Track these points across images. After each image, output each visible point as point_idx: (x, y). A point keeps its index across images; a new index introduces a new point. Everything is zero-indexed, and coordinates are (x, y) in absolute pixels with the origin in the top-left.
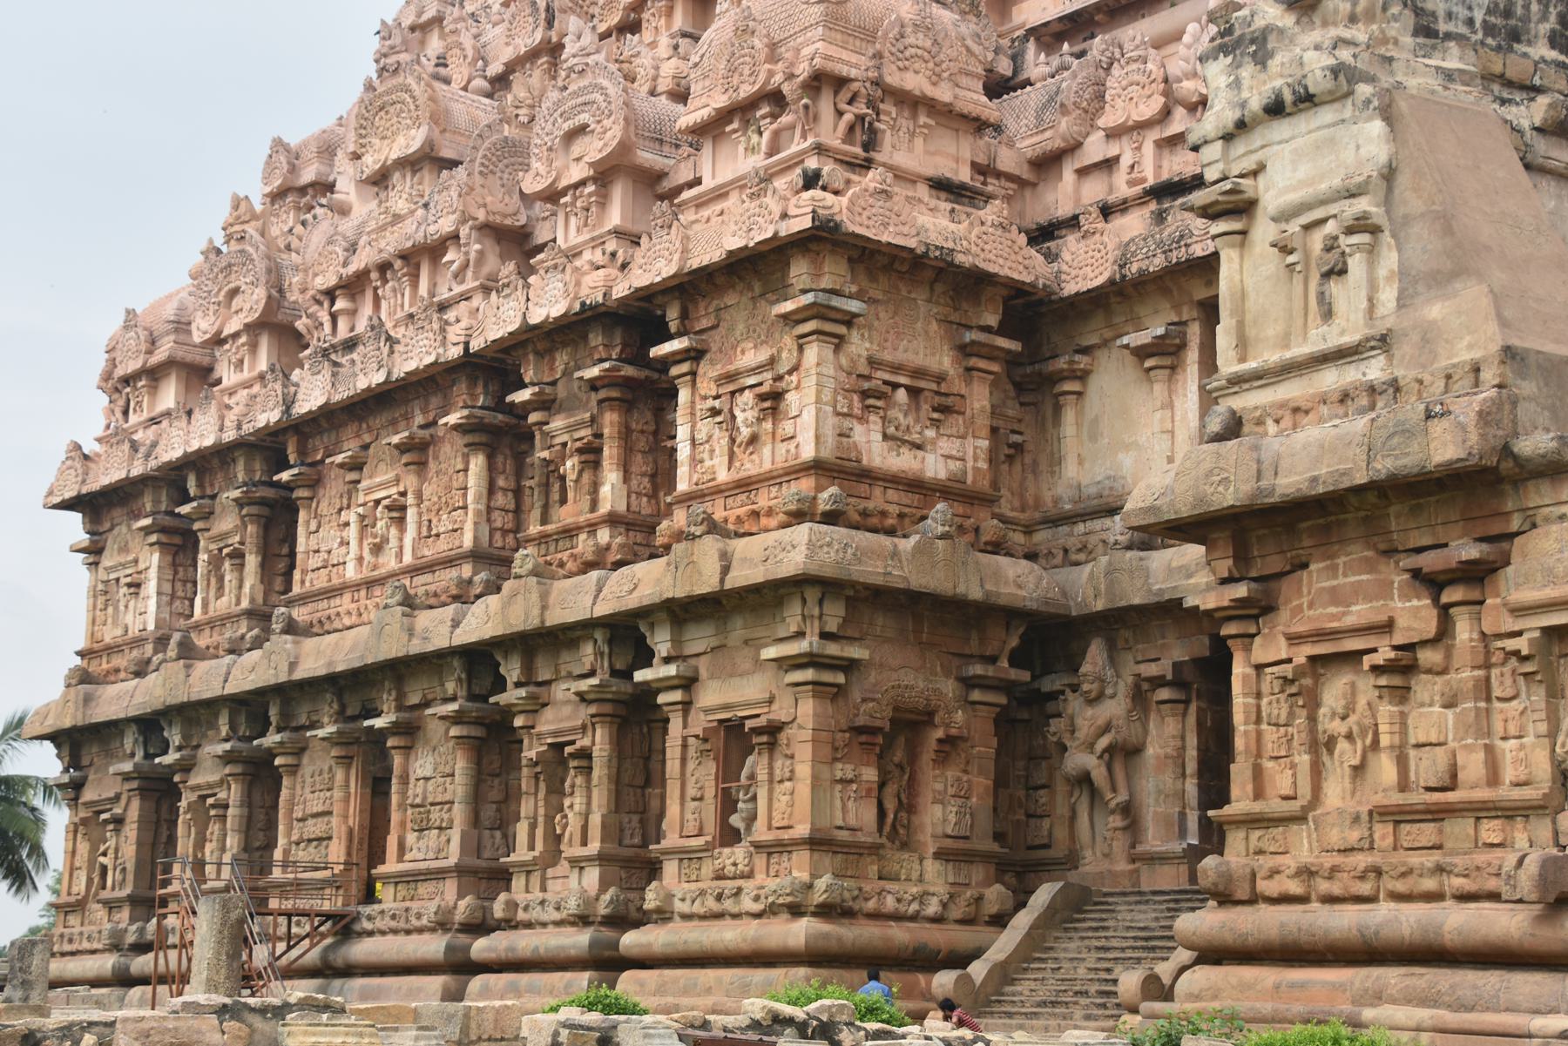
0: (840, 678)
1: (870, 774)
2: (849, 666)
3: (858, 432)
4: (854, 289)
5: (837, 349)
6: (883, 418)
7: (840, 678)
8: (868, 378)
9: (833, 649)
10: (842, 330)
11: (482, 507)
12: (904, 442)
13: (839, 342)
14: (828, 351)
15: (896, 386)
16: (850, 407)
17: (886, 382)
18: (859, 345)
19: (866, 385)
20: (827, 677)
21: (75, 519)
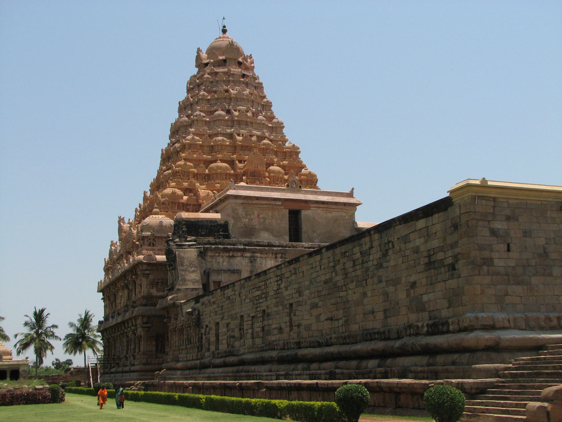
0: (147, 329)
1: (154, 343)
2: (149, 327)
3: (152, 291)
4: (150, 268)
5: (147, 279)
6: (157, 288)
7: (147, 329)
8: (153, 282)
9: (144, 325)
10: (147, 276)
11: (127, 298)
12: (160, 291)
13: (147, 278)
14: (145, 279)
15: (159, 282)
16: (150, 287)
17: (157, 282)
18: (151, 277)
19: (152, 283)
20: (145, 329)
21: (101, 293)
